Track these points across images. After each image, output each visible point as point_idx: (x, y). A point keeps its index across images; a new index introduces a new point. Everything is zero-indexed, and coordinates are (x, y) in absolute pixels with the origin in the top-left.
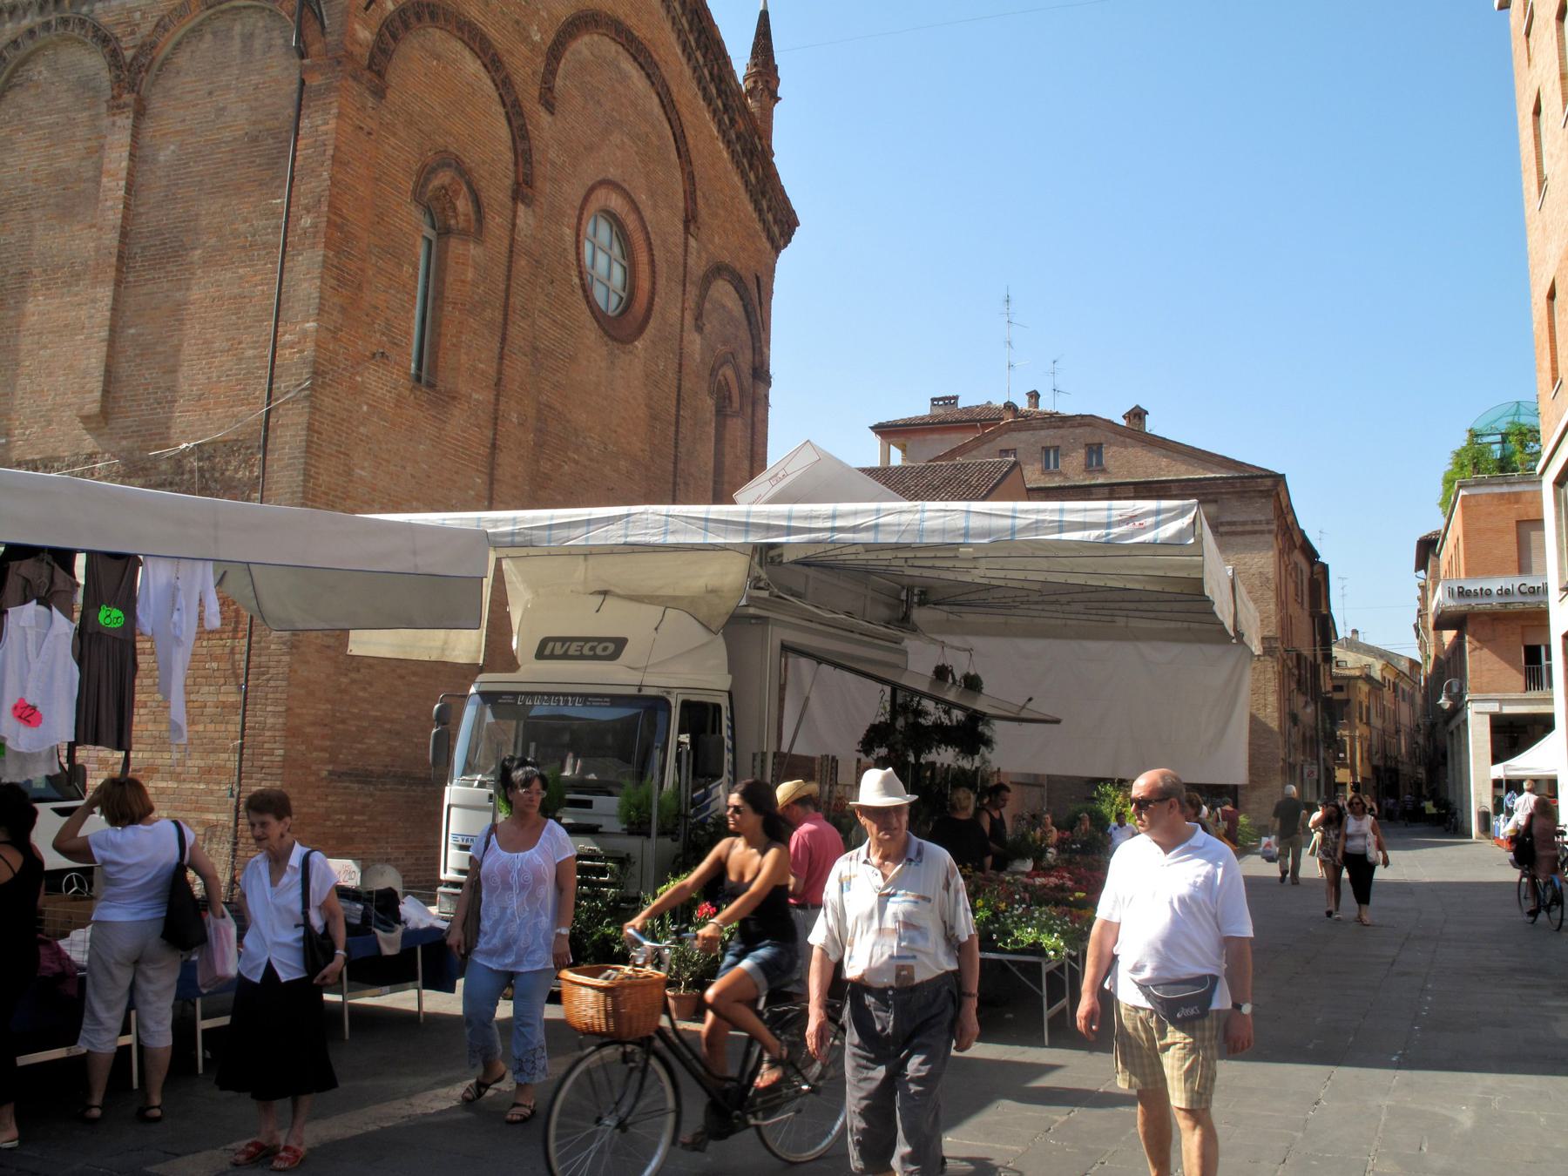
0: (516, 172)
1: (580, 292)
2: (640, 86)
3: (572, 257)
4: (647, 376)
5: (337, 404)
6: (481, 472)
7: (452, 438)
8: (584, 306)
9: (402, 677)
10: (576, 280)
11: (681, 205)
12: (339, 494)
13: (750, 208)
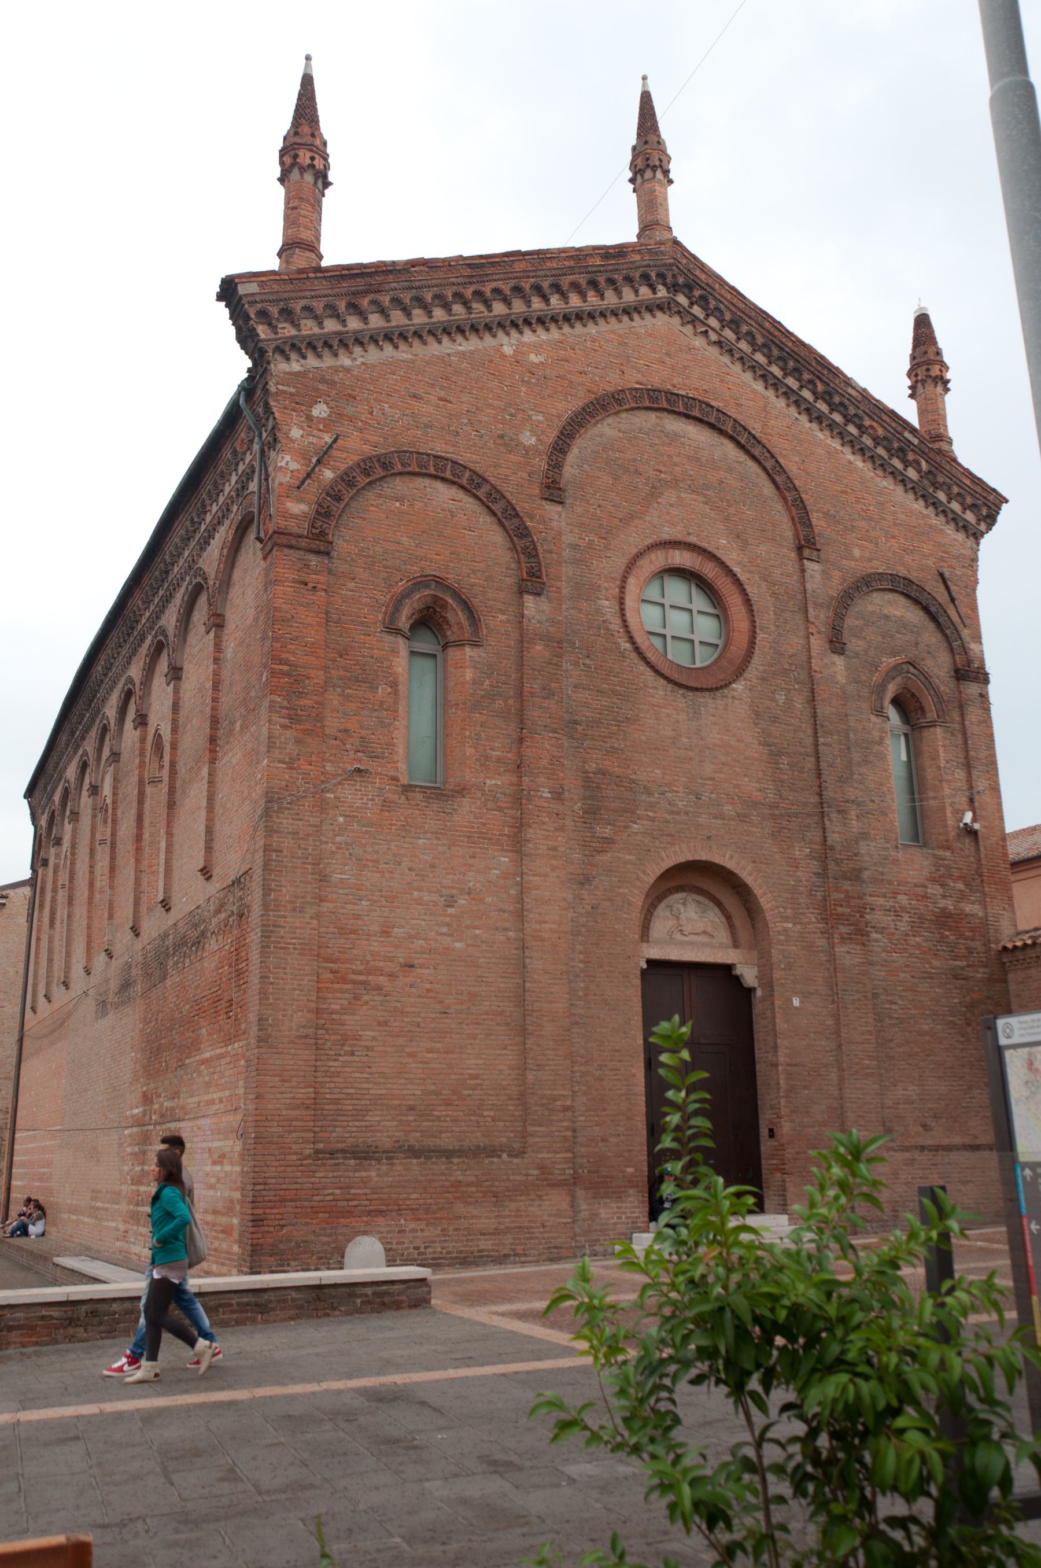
0: (520, 568)
1: (634, 655)
2: (703, 438)
3: (616, 624)
4: (757, 714)
5: (300, 823)
6: (507, 851)
7: (466, 827)
8: (642, 667)
9: (412, 1055)
10: (628, 646)
11: (789, 534)
12: (309, 899)
13: (919, 506)
